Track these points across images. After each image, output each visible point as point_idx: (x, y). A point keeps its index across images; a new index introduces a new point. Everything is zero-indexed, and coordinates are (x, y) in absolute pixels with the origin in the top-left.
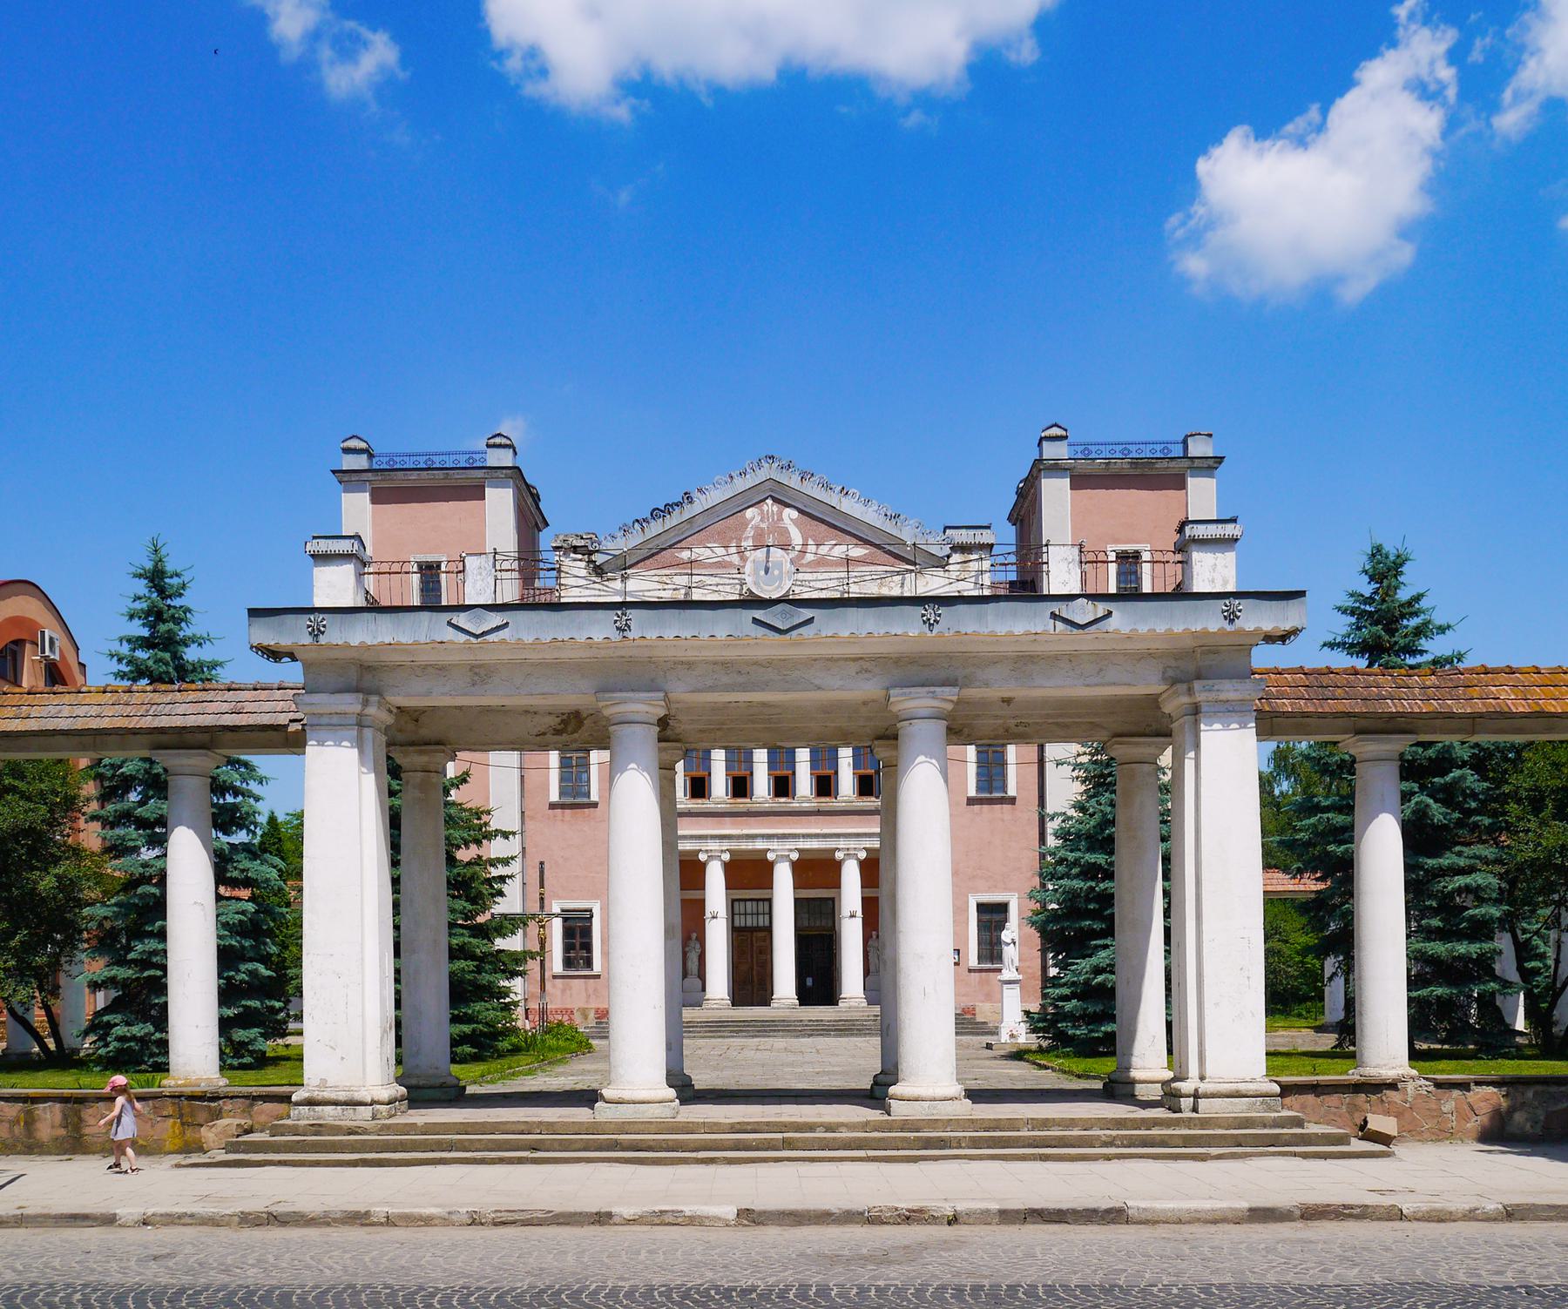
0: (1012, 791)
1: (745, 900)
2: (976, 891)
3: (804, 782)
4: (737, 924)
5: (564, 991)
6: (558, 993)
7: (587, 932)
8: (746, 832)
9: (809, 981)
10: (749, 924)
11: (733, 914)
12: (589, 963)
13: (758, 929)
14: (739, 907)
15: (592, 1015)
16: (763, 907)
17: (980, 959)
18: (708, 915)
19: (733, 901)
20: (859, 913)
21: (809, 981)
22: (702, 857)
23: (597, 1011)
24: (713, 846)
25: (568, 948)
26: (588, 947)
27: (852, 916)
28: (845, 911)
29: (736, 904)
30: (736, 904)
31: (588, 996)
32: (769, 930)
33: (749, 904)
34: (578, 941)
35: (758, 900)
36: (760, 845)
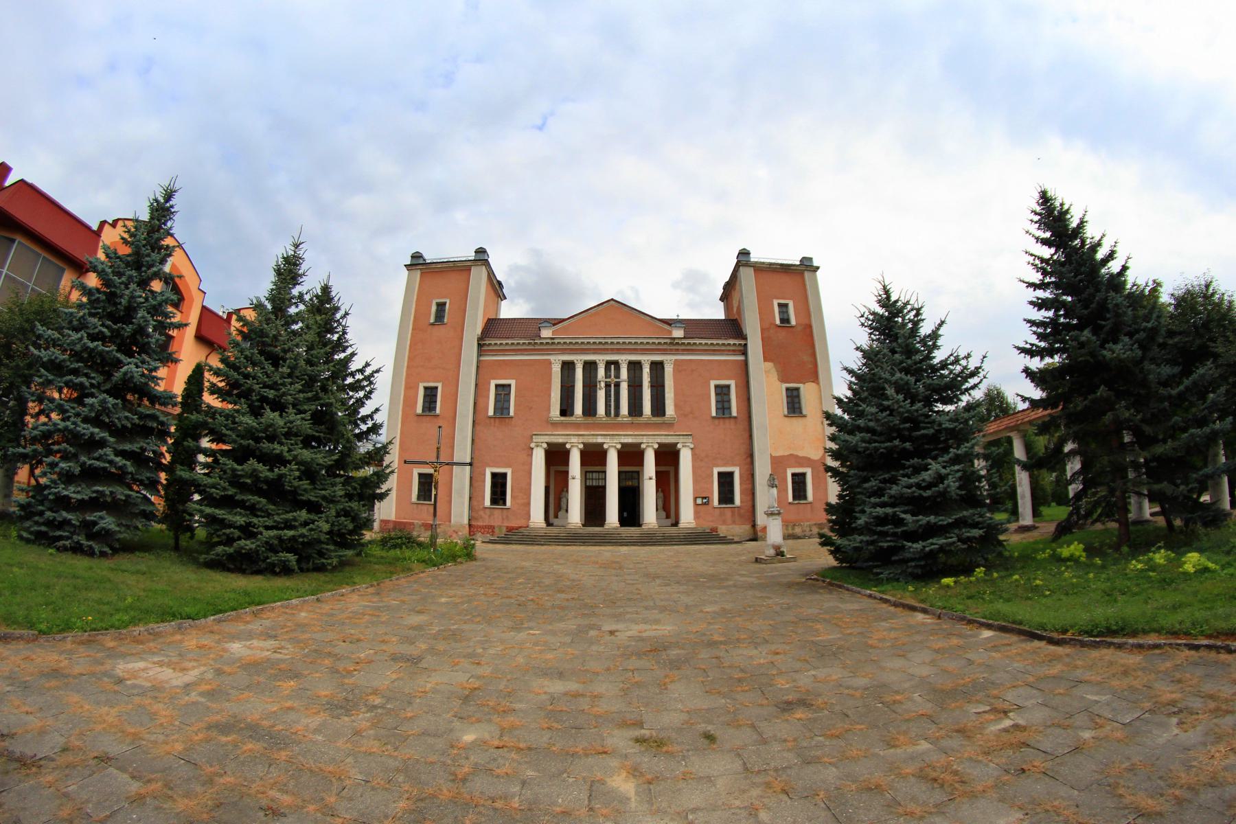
0: (734, 413)
1: (592, 472)
2: (718, 466)
3: (624, 409)
4: (588, 484)
5: (490, 516)
6: (487, 517)
7: (504, 485)
8: (592, 433)
9: (625, 514)
10: (594, 484)
11: (586, 479)
12: (504, 503)
13: (599, 487)
14: (589, 475)
15: (504, 530)
16: (601, 476)
17: (720, 502)
18: (570, 477)
19: (586, 472)
20: (654, 477)
21: (625, 514)
22: (568, 446)
23: (507, 527)
24: (574, 440)
25: (493, 493)
26: (504, 493)
27: (651, 479)
28: (646, 475)
29: (588, 474)
30: (588, 474)
31: (503, 519)
32: (604, 487)
33: (594, 474)
34: (499, 490)
35: (599, 472)
36: (600, 440)
